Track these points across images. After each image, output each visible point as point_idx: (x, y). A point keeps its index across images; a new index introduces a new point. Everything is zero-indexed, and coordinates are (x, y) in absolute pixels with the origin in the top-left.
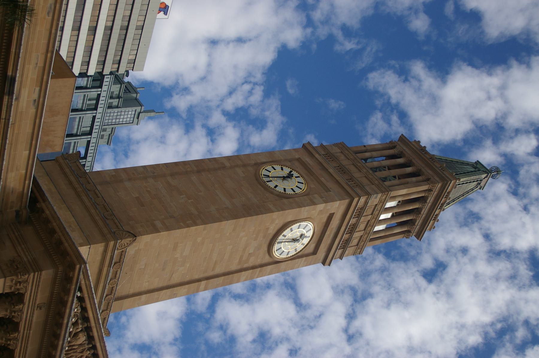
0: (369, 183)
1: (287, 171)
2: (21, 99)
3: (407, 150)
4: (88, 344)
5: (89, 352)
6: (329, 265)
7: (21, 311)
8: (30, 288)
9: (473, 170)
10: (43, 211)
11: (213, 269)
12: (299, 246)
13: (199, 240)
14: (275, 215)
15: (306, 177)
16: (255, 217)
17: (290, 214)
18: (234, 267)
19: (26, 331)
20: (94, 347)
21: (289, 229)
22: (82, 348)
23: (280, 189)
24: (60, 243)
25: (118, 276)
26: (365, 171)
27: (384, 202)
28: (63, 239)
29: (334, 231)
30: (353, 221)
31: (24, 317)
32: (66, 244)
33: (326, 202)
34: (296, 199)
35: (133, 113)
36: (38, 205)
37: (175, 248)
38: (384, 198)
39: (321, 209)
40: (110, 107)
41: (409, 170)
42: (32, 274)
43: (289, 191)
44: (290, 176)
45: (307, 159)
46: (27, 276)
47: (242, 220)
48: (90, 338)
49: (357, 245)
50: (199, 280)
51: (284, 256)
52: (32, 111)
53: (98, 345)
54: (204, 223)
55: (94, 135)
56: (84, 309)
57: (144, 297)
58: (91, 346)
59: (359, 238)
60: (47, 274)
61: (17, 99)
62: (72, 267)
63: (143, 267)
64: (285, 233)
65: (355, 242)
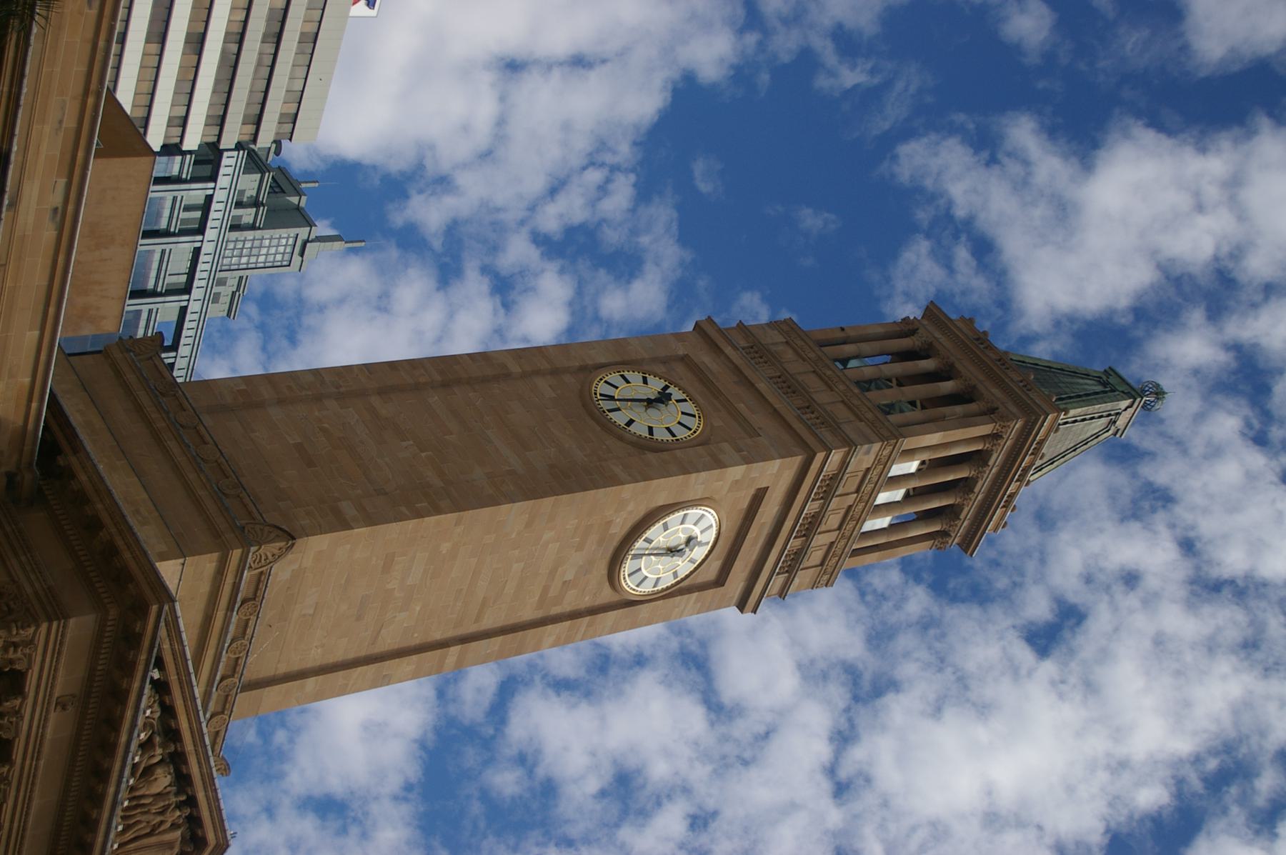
0: (852, 418)
1: (656, 385)
2: (22, 207)
3: (943, 339)
4: (177, 794)
5: (178, 813)
6: (754, 611)
7: (18, 713)
8: (39, 659)
9: (1099, 388)
10: (73, 476)
12: (683, 566)
13: (445, 547)
14: (627, 490)
15: (701, 401)
16: (578, 496)
17: (661, 490)
18: (528, 614)
19: (28, 762)
20: (192, 802)
21: (659, 525)
22: (162, 804)
23: (640, 429)
24: (111, 551)
25: (249, 631)
26: (842, 387)
27: (887, 463)
28: (120, 543)
29: (766, 531)
30: (812, 507)
31: (25, 727)
32: (127, 555)
33: (748, 461)
34: (678, 453)
35: (291, 241)
36: (61, 461)
37: (387, 566)
38: (886, 452)
39: (737, 479)
40: (235, 227)
41: (947, 387)
42: (44, 626)
43: (661, 435)
44: (663, 398)
45: (705, 358)
46: (32, 630)
47: (548, 502)
48: (182, 780)
49: (822, 564)
50: (444, 644)
51: (647, 588)
52: (49, 234)
53: (201, 796)
54: (458, 507)
55: (196, 293)
56: (168, 711)
57: (311, 683)
58: (183, 798)
59: (825, 548)
60: (80, 627)
62: (140, 609)
63: (311, 612)
64: (648, 534)
65: (815, 556)
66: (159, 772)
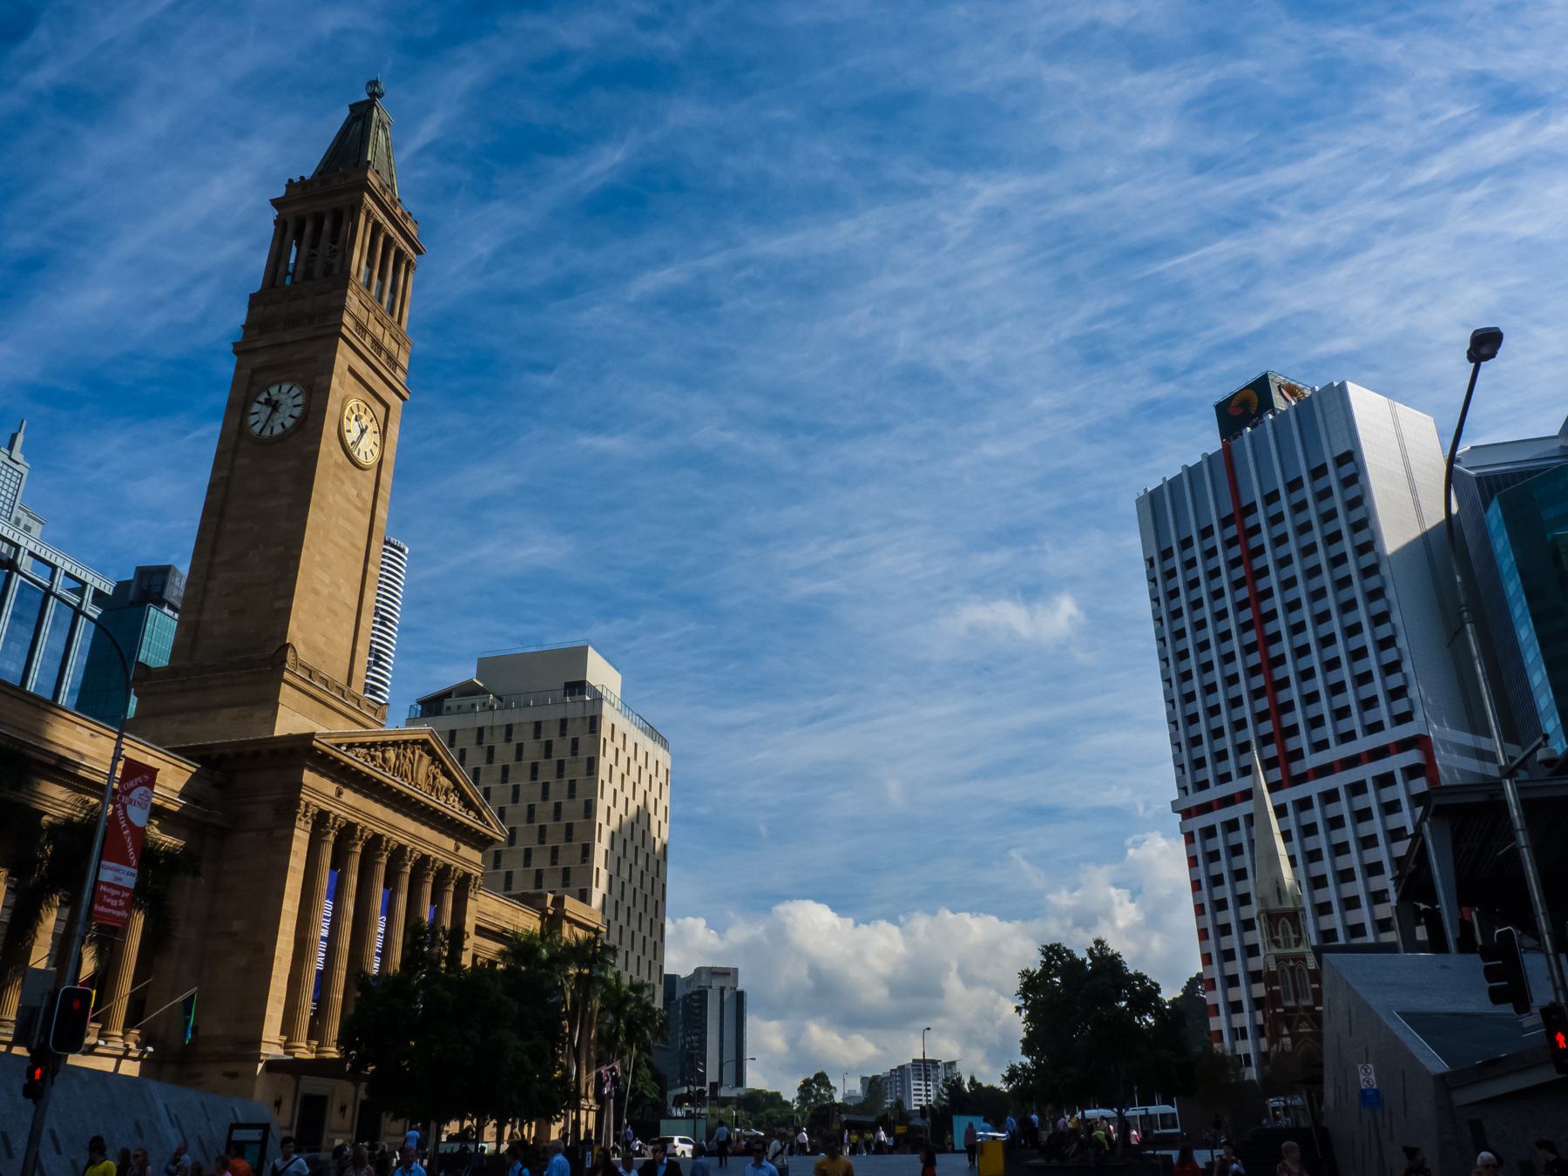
11: (358, 548)
12: (372, 427)
13: (317, 558)
17: (329, 429)
20: (405, 742)
23: (289, 422)
33: (331, 372)
37: (316, 592)
39: (340, 383)
41: (327, 225)
43: (297, 412)
45: (259, 360)
51: (376, 451)
55: (22, 542)
56: (362, 745)
60: (309, 777)
61: (82, 756)
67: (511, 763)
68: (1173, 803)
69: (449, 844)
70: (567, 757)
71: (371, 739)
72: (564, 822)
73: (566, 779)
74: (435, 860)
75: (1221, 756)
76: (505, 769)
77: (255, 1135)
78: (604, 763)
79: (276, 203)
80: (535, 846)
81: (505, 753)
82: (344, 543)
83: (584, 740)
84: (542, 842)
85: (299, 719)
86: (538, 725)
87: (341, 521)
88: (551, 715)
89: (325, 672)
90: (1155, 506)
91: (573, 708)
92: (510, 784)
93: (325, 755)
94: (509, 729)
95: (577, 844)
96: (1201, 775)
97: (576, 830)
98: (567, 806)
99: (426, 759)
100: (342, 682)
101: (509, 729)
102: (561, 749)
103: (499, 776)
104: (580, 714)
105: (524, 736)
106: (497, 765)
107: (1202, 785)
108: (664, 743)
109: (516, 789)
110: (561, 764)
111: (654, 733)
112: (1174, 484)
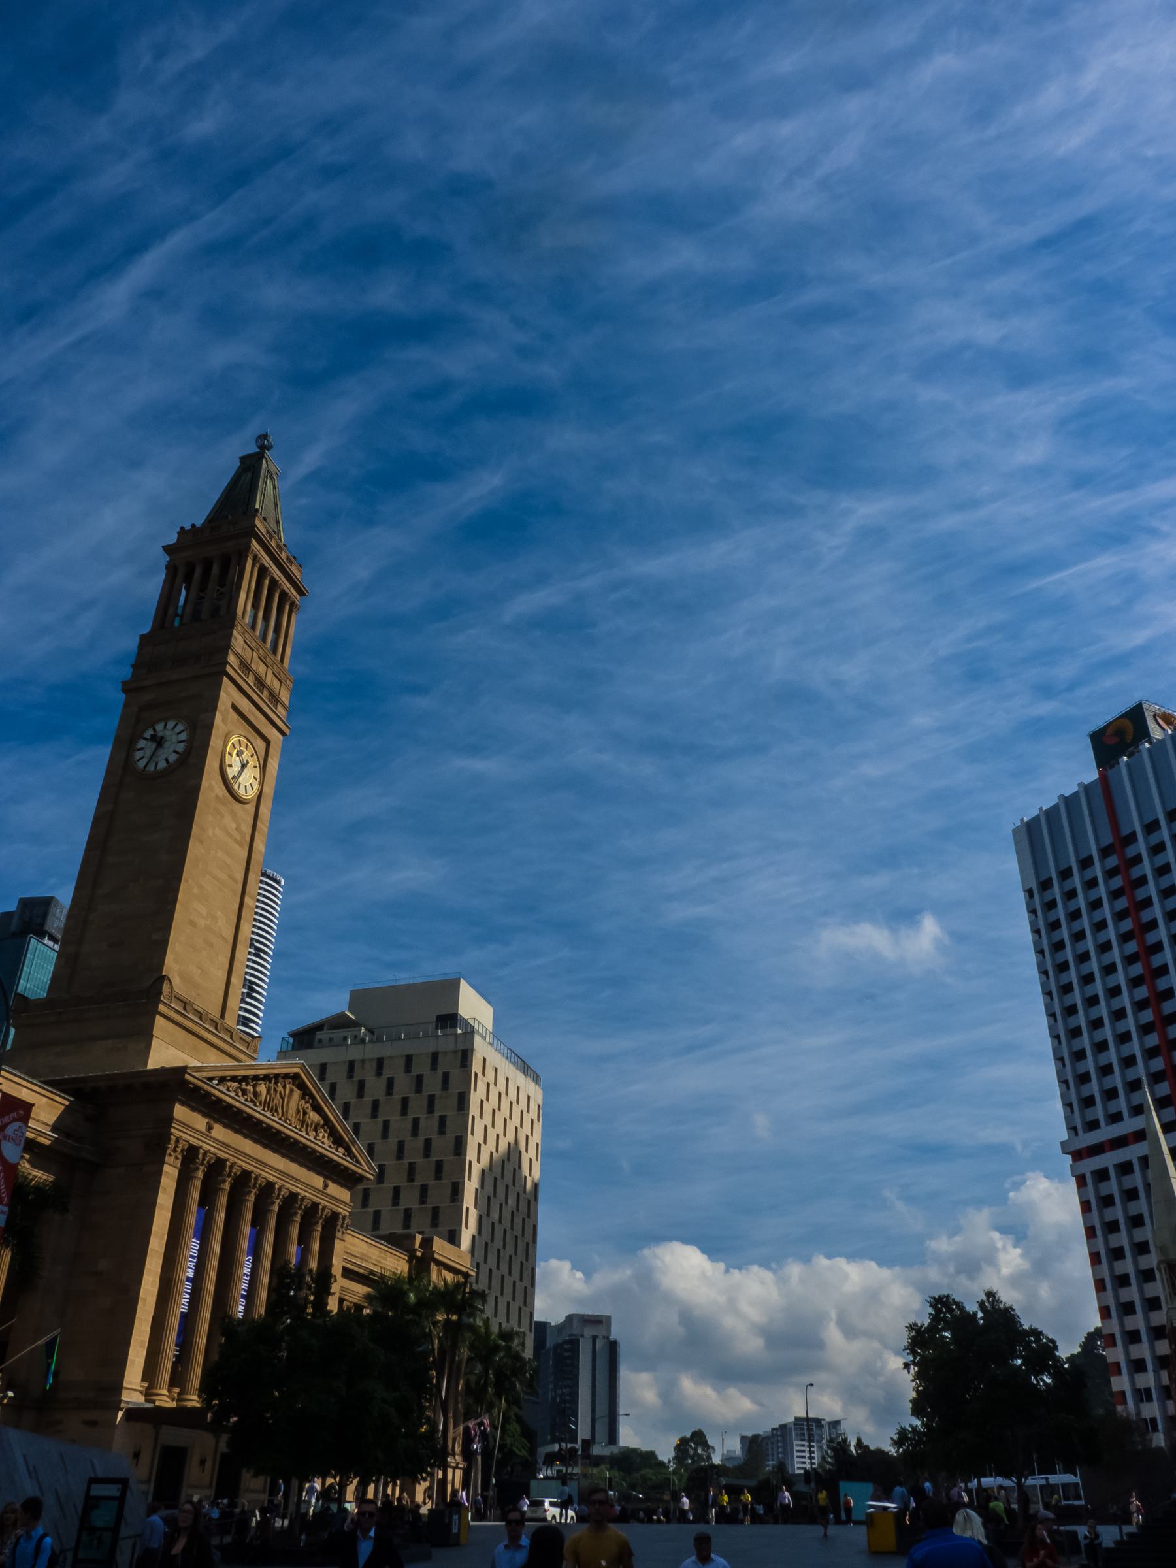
9: (249, 475)
12: (253, 762)
13: (196, 891)
14: (204, 783)
17: (211, 763)
20: (277, 1076)
23: (173, 758)
30: (251, 679)
37: (193, 924)
39: (223, 720)
41: (215, 569)
43: (181, 748)
47: (195, 829)
51: (256, 785)
54: (178, 878)
56: (234, 1079)
60: (180, 1111)
64: (230, 776)
66: (258, 1089)
67: (382, 1097)
68: (1063, 1144)
69: (318, 1181)
70: (438, 1092)
71: (242, 1073)
72: (434, 1159)
73: (437, 1115)
74: (304, 1198)
75: (1111, 1094)
76: (375, 1105)
77: (113, 1490)
78: (475, 1098)
79: (168, 549)
80: (404, 1184)
81: (375, 1088)
82: (222, 876)
83: (455, 1073)
84: (411, 1179)
85: (172, 1051)
86: (409, 1059)
87: (220, 854)
88: (422, 1048)
89: (199, 1005)
90: (1035, 836)
91: (444, 1042)
92: (380, 1120)
93: (197, 1089)
94: (380, 1063)
95: (446, 1181)
96: (1090, 1114)
97: (445, 1168)
98: (437, 1142)
99: (297, 1094)
100: (215, 1013)
101: (380, 1063)
102: (432, 1084)
103: (369, 1111)
104: (451, 1047)
105: (394, 1070)
106: (368, 1099)
107: (1093, 1125)
108: (536, 1078)
109: (386, 1124)
110: (431, 1100)
111: (526, 1068)
112: (1051, 814)
